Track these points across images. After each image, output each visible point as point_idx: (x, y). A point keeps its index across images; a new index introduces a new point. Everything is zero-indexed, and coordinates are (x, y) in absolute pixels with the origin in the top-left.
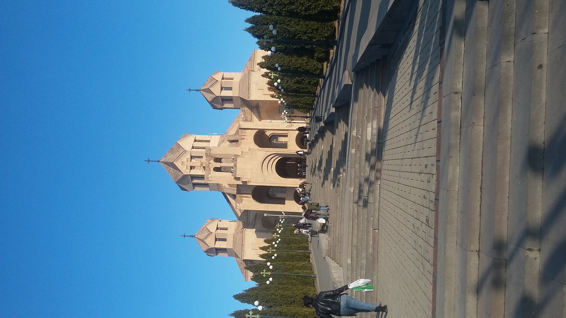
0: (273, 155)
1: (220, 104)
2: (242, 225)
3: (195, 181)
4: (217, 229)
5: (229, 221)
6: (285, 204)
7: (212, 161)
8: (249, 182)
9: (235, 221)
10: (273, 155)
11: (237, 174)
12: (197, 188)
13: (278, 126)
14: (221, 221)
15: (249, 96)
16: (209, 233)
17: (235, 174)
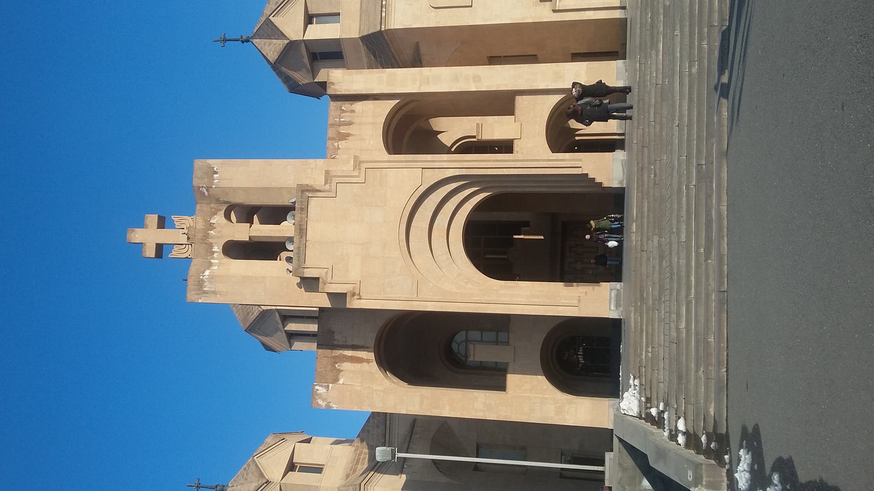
0: (454, 185)
1: (304, 70)
2: (367, 458)
3: (292, 327)
4: (291, 467)
5: (333, 439)
6: (505, 390)
7: (219, 219)
8: (353, 295)
9: (350, 442)
10: (454, 185)
11: (308, 263)
12: (298, 345)
13: (477, 79)
14: (308, 441)
15: (384, 14)
16: (260, 483)
17: (301, 266)
